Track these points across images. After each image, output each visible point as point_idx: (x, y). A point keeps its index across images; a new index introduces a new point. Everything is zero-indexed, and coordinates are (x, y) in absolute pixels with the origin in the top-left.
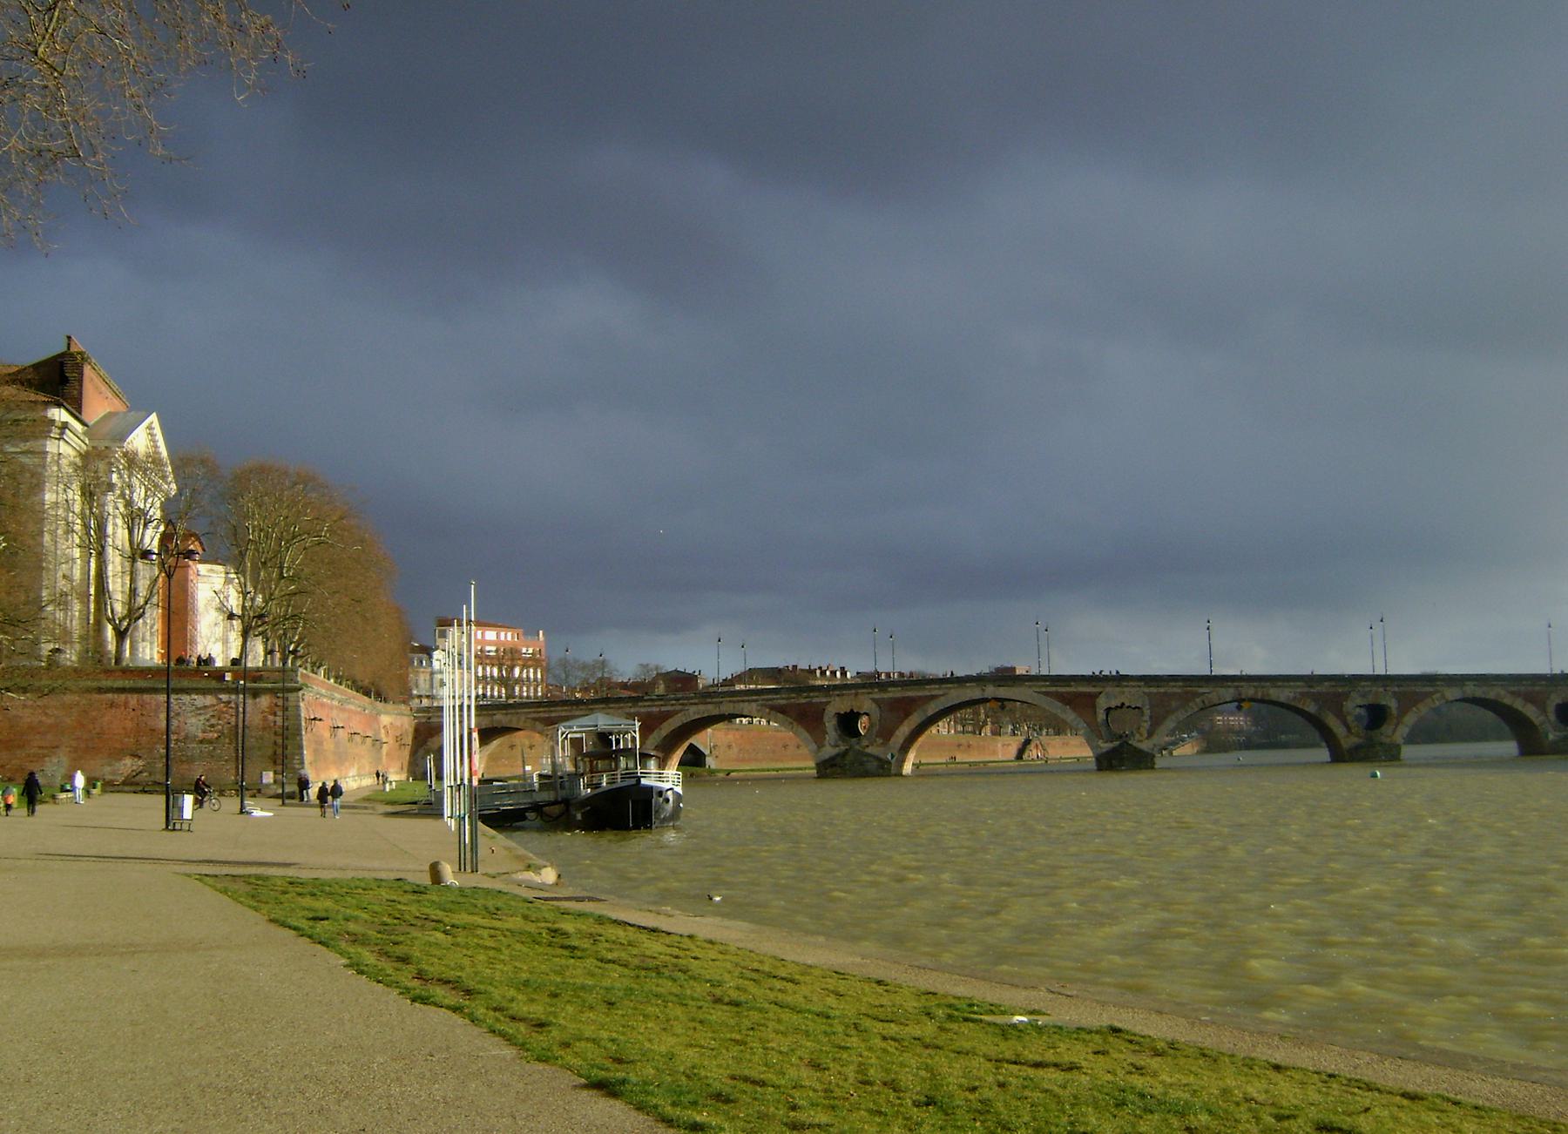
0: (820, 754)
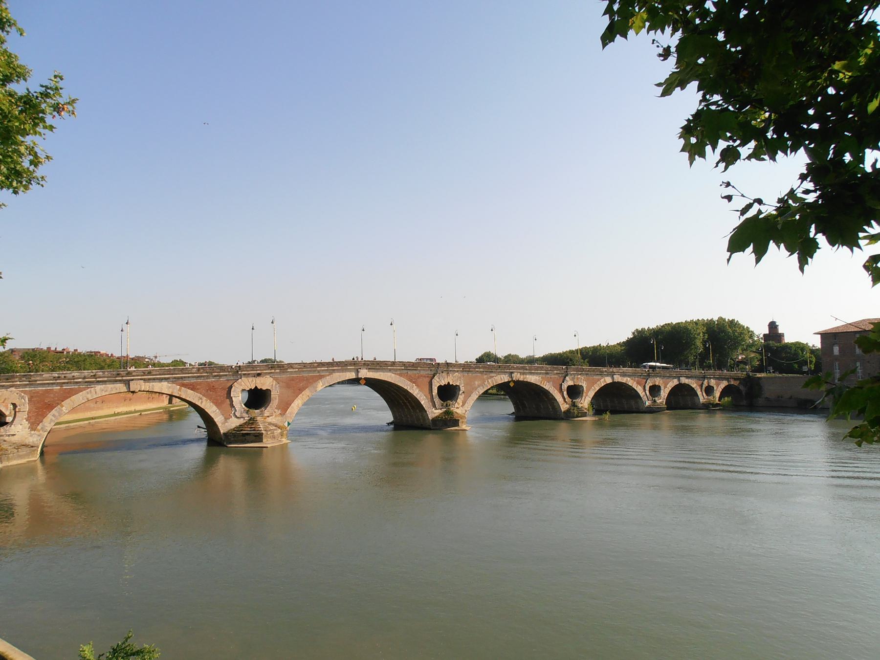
0: (226, 424)
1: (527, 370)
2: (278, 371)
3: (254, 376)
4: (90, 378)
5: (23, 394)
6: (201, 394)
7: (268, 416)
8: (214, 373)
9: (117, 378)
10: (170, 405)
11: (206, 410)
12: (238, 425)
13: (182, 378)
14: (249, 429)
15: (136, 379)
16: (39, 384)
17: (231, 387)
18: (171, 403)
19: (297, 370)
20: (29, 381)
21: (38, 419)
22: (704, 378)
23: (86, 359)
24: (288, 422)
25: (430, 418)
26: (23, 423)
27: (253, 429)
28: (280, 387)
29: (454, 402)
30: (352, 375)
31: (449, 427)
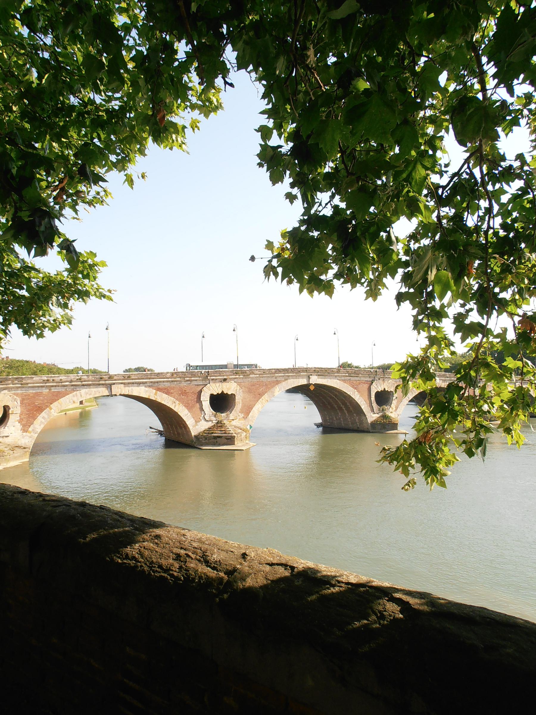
1: (448, 377)
2: (242, 376)
3: (221, 381)
4: (77, 382)
5: (15, 397)
6: (174, 397)
7: (233, 420)
8: (186, 377)
9: (101, 382)
10: (81, 405)
11: (179, 413)
12: (207, 427)
13: (157, 382)
14: (219, 432)
15: (117, 383)
16: (30, 387)
17: (201, 391)
18: (82, 404)
19: (258, 376)
20: (21, 384)
21: (29, 421)
23: (24, 365)
24: (250, 425)
25: (369, 422)
26: (16, 425)
27: (224, 432)
28: (243, 392)
29: (389, 407)
30: (303, 381)
31: (388, 431)
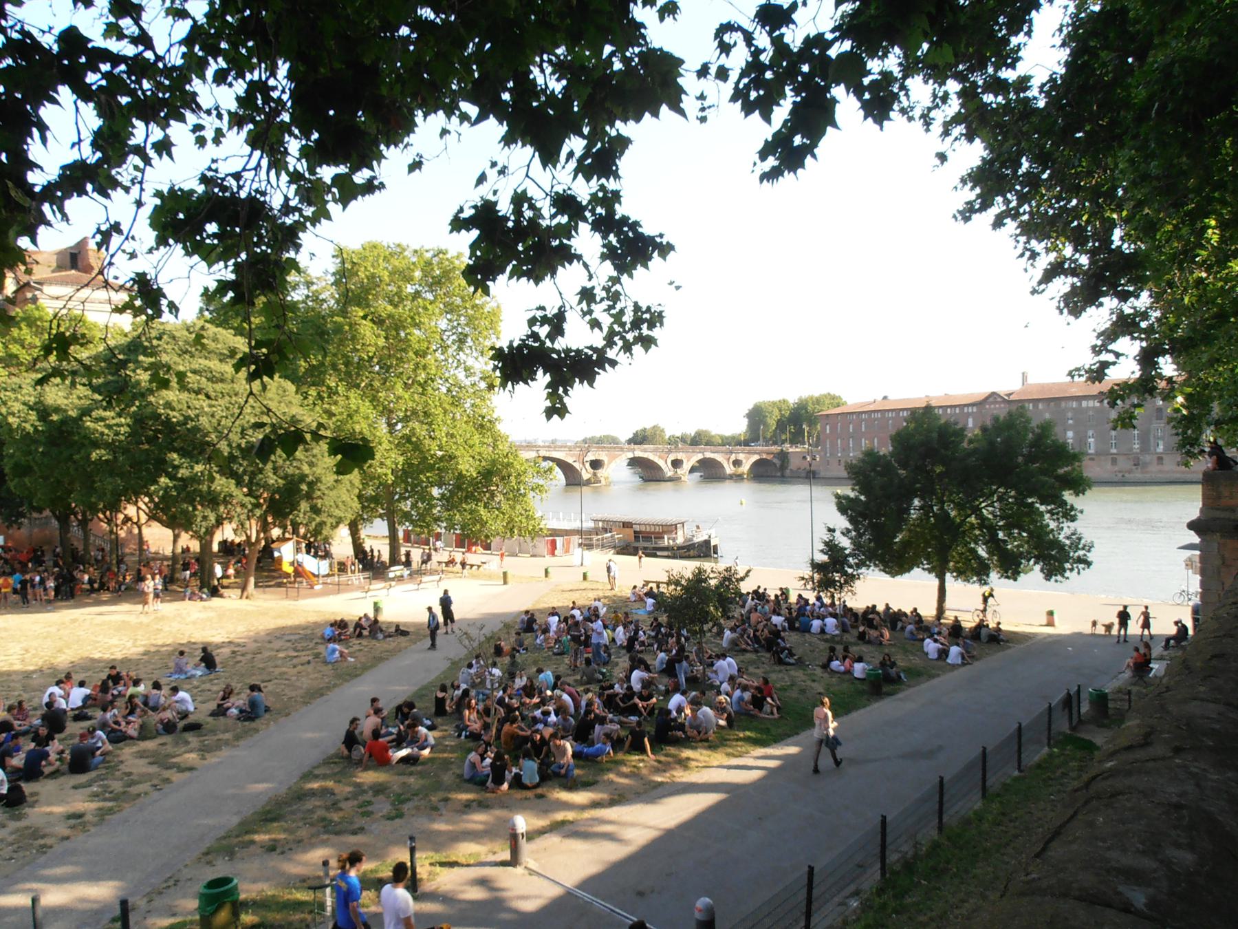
22: (731, 452)
